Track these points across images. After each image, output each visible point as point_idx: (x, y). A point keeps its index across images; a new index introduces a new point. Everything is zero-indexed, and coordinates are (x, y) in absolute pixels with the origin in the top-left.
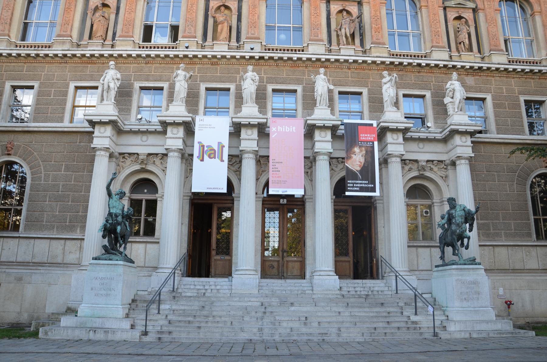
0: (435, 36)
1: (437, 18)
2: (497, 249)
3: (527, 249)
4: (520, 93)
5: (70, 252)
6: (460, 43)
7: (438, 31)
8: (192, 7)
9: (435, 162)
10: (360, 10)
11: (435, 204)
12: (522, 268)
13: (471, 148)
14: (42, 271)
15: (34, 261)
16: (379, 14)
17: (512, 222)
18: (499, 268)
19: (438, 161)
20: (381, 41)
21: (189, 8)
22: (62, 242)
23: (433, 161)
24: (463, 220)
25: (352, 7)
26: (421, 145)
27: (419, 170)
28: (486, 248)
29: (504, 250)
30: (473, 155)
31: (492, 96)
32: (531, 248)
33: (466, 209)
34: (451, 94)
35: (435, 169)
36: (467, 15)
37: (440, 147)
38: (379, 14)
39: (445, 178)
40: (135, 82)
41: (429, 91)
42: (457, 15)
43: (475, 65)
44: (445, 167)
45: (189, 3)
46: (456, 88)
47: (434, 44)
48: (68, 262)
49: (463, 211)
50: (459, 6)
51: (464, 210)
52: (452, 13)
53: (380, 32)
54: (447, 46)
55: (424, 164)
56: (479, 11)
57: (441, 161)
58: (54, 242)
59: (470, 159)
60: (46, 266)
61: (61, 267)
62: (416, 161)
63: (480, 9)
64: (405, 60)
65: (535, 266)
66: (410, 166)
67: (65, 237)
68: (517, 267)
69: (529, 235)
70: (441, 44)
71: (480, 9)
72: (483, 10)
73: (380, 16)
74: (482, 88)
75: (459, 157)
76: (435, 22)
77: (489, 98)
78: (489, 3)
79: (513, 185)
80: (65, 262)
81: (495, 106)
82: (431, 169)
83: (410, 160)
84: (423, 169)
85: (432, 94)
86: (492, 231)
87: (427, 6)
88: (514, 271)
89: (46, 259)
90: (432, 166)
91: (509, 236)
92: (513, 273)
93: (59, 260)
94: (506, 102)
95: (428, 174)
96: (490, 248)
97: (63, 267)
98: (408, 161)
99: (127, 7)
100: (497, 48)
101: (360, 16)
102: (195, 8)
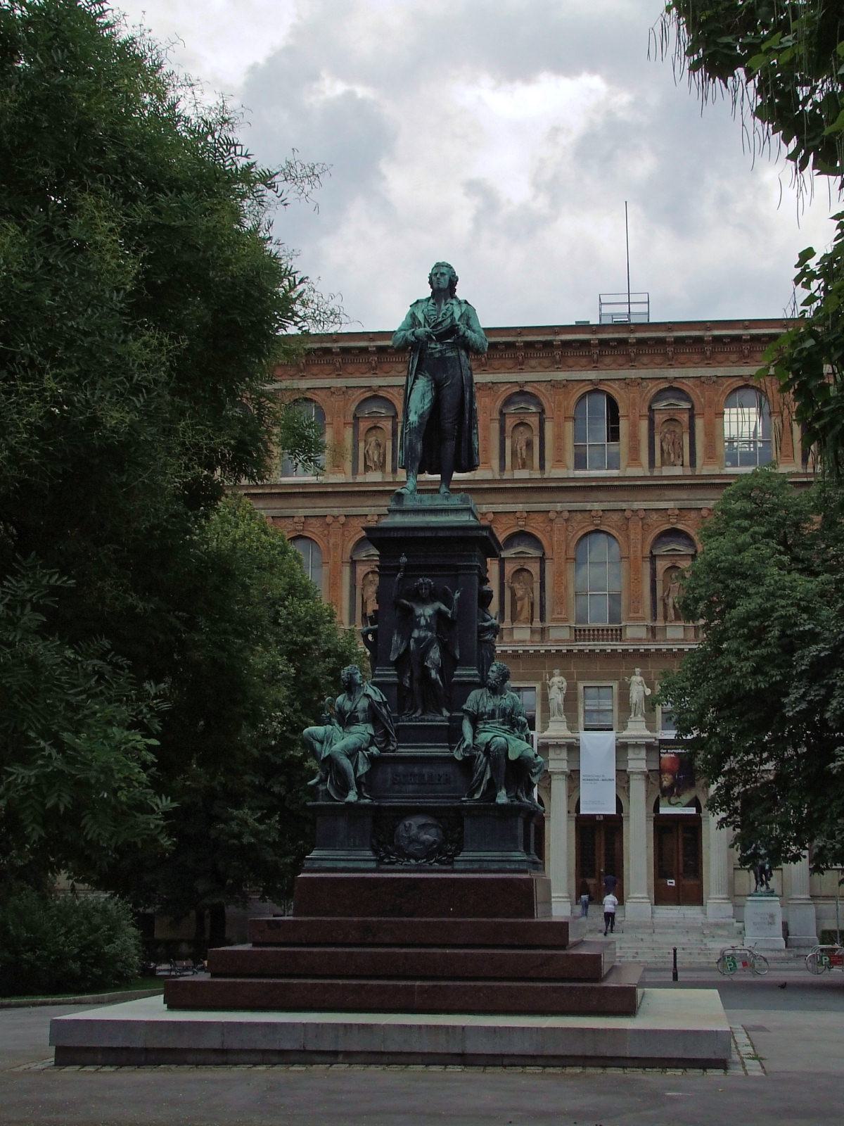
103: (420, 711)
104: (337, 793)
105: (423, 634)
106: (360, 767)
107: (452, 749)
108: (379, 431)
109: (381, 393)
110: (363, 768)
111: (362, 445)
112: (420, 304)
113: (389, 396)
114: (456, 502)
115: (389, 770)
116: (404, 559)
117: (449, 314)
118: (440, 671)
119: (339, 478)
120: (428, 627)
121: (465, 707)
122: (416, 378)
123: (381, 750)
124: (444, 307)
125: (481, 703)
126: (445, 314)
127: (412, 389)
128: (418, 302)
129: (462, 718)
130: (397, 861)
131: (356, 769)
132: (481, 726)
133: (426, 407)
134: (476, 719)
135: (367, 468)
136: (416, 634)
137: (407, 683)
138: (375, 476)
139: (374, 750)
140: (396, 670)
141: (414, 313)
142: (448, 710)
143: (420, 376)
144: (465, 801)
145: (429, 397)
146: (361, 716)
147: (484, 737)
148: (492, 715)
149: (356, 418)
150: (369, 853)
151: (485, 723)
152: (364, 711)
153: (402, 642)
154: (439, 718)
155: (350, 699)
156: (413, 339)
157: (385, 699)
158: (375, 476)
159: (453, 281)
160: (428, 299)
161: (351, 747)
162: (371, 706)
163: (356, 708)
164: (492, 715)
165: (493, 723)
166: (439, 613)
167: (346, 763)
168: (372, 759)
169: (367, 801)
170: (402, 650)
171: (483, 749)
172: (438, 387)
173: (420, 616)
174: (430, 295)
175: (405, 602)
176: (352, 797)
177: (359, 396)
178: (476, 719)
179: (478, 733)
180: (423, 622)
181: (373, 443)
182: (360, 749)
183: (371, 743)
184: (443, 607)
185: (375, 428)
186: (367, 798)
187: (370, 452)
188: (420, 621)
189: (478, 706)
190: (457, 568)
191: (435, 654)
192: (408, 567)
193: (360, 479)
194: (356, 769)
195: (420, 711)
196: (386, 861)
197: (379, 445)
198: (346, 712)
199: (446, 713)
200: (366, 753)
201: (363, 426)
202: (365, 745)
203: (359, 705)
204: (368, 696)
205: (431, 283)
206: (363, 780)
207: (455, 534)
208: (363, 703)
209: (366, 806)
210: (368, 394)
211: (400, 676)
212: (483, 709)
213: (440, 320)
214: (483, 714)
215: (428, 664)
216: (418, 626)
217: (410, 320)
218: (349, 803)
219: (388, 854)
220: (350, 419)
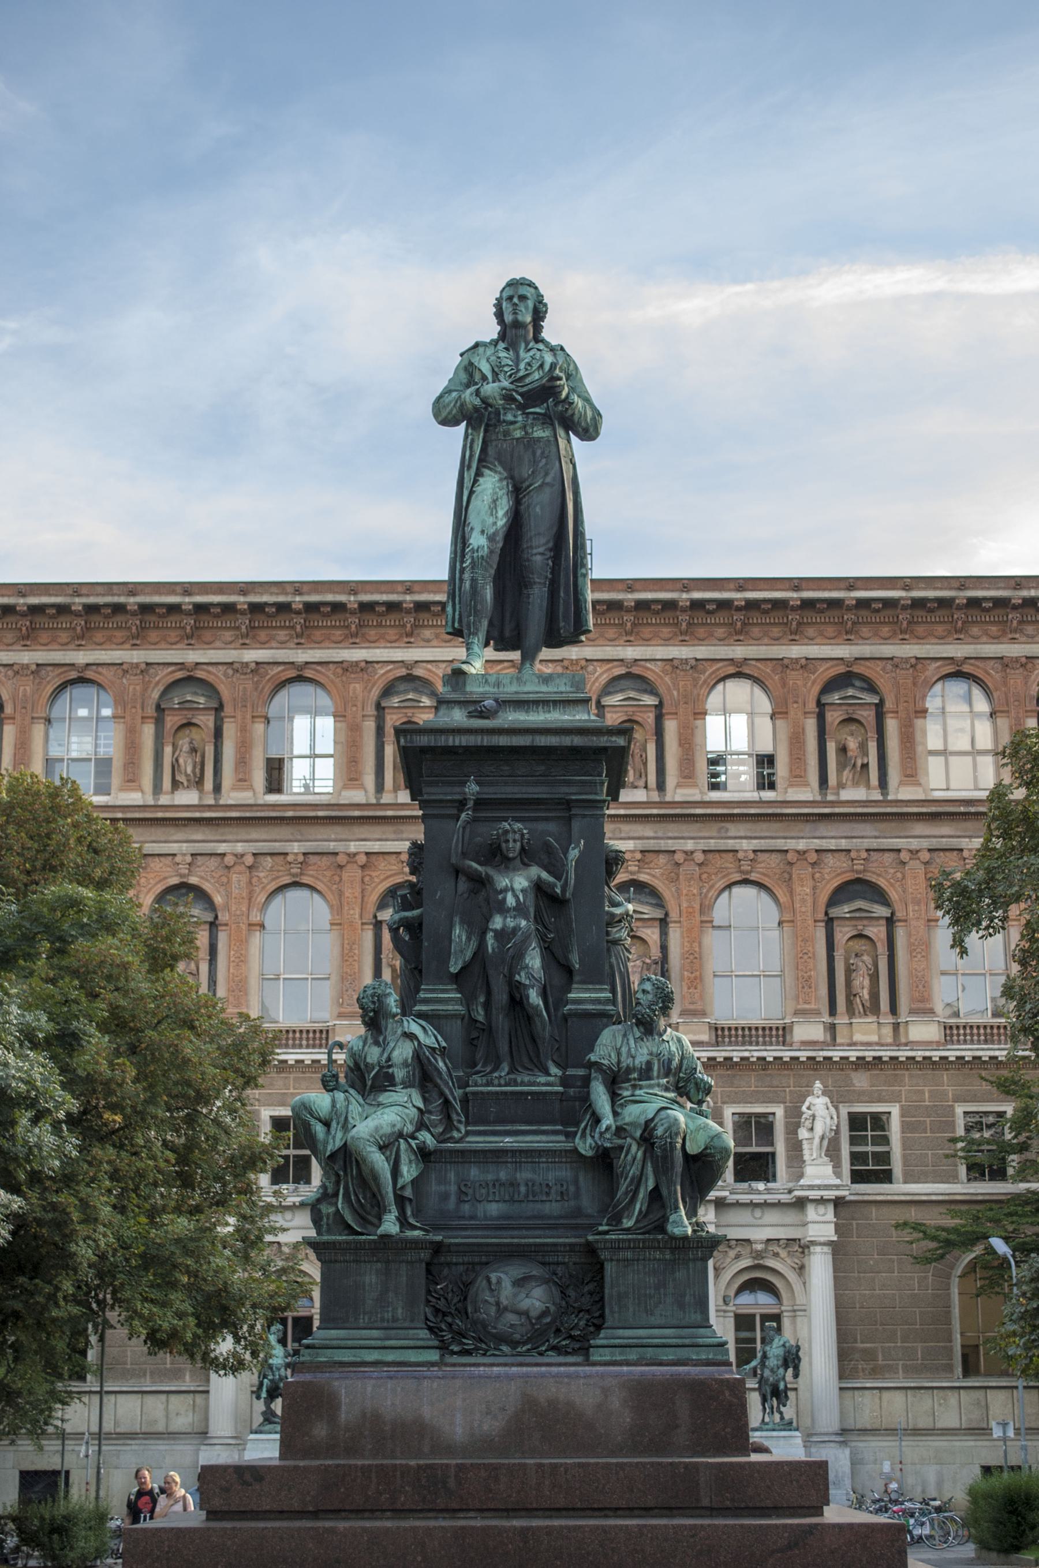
0: (803, 987)
1: (810, 949)
2: (886, 1395)
3: (942, 1393)
4: (959, 1099)
5: (177, 1414)
6: (855, 995)
7: (810, 977)
8: (351, 949)
9: (781, 1242)
10: (664, 934)
11: (785, 1314)
12: (931, 1426)
13: (833, 1225)
14: (134, 1447)
15: (118, 1430)
16: (697, 949)
17: (919, 1346)
18: (889, 1427)
19: (788, 1240)
20: (698, 1006)
21: (346, 952)
22: (163, 1397)
23: (778, 1240)
24: (780, 1363)
25: (649, 931)
26: (758, 1213)
27: (754, 1258)
28: (867, 1392)
29: (898, 1397)
30: (835, 1238)
31: (902, 1108)
32: (949, 1393)
33: (787, 1345)
34: (808, 1124)
35: (783, 1254)
36: (875, 930)
37: (791, 1217)
38: (697, 949)
39: (801, 1269)
40: (262, 1109)
41: (782, 1105)
42: (855, 933)
43: (867, 1054)
44: (800, 1250)
45: (346, 942)
46: (817, 1114)
47: (799, 1007)
48: (176, 1431)
49: (782, 1349)
50: (857, 915)
51: (784, 1346)
52: (846, 929)
53: (699, 986)
54: (825, 1008)
55: (759, 1247)
56: (898, 924)
57: (794, 1240)
58: (150, 1399)
59: (830, 1243)
60: (139, 1439)
61: (164, 1439)
62: (748, 1241)
63: (899, 921)
64: (735, 1054)
65: (955, 1424)
66: (738, 1249)
67: (167, 1389)
68: (921, 1425)
69: (949, 1368)
70: (813, 1006)
71: (899, 921)
72: (906, 921)
73: (700, 953)
74: (884, 1094)
75: (813, 1243)
76: (806, 957)
77: (895, 1110)
78: (916, 908)
79: (926, 1278)
80: (170, 1430)
81: (906, 1127)
82: (776, 1255)
83: (737, 1240)
84: (759, 1255)
85: (786, 1112)
86: (880, 1362)
87: (792, 921)
88: (916, 1432)
89: (138, 1426)
90: (777, 1249)
91: (911, 1371)
92: (914, 1435)
93: (160, 1427)
94: (928, 1120)
95: (771, 1263)
96: (874, 1392)
97: (168, 1439)
98: (734, 1242)
99: (232, 953)
100: (921, 1005)
101: (664, 948)
102: (356, 951)
103: (505, 1067)
104: (363, 1220)
105: (511, 923)
106: (404, 1169)
107: (570, 1136)
108: (194, 729)
109: (200, 674)
110: (409, 1172)
111: (168, 750)
112: (481, 349)
113: (210, 679)
114: (563, 689)
115: (452, 1176)
116: (472, 788)
117: (535, 366)
118: (544, 994)
119: (134, 798)
120: (520, 910)
121: (593, 1057)
122: (479, 474)
123: (440, 1139)
124: (525, 356)
125: (624, 1050)
126: (529, 364)
127: (471, 492)
128: (477, 345)
129: (586, 1081)
130: (477, 1349)
131: (396, 1172)
132: (626, 1093)
133: (501, 523)
134: (615, 1080)
135: (176, 785)
136: (497, 922)
137: (480, 1015)
138: (188, 797)
139: (426, 1137)
140: (459, 991)
141: (471, 364)
142: (558, 1065)
143: (487, 472)
144: (606, 1233)
145: (504, 507)
146: (400, 1074)
147: (633, 1113)
148: (646, 1073)
149: (159, 708)
150: (424, 1333)
151: (634, 1087)
152: (405, 1064)
153: (469, 939)
154: (542, 1079)
155: (377, 1043)
156: (477, 402)
157: (444, 1044)
158: (188, 797)
159: (539, 314)
160: (495, 343)
161: (388, 1130)
162: (417, 1056)
163: (389, 1059)
164: (646, 1073)
165: (651, 1087)
166: (539, 888)
167: (379, 1161)
168: (424, 1154)
169: (416, 1233)
170: (469, 954)
171: (638, 1134)
172: (518, 491)
173: (505, 890)
174: (495, 336)
175: (475, 865)
176: (390, 1225)
177: (163, 677)
178: (615, 1080)
179: (622, 1106)
180: (510, 901)
181: (186, 748)
182: (400, 1135)
183: (421, 1125)
184: (544, 875)
185: (189, 724)
186: (415, 1228)
187: (181, 761)
188: (505, 899)
189: (619, 1054)
190: (567, 804)
191: (534, 960)
192: (480, 803)
193: (164, 800)
194: (396, 1172)
195: (505, 1067)
196: (456, 1348)
197: (194, 750)
198: (369, 1067)
199: (554, 1070)
200: (413, 1143)
201: (171, 721)
202: (409, 1128)
203: (395, 1054)
204: (410, 1036)
205: (499, 315)
206: (408, 1193)
207: (567, 741)
208: (403, 1052)
209: (415, 1244)
210: (179, 675)
211: (468, 1000)
212: (630, 1061)
213: (521, 374)
214: (629, 1070)
215: (522, 978)
216: (501, 908)
217: (463, 377)
218: (386, 1237)
219: (460, 1335)
220: (151, 711)
